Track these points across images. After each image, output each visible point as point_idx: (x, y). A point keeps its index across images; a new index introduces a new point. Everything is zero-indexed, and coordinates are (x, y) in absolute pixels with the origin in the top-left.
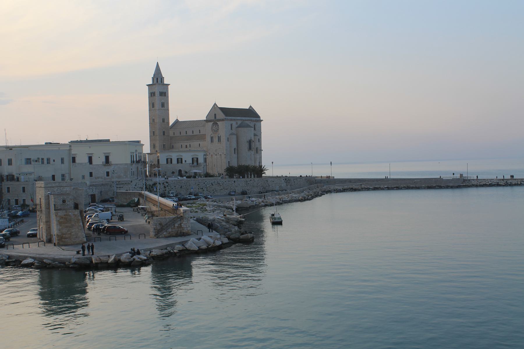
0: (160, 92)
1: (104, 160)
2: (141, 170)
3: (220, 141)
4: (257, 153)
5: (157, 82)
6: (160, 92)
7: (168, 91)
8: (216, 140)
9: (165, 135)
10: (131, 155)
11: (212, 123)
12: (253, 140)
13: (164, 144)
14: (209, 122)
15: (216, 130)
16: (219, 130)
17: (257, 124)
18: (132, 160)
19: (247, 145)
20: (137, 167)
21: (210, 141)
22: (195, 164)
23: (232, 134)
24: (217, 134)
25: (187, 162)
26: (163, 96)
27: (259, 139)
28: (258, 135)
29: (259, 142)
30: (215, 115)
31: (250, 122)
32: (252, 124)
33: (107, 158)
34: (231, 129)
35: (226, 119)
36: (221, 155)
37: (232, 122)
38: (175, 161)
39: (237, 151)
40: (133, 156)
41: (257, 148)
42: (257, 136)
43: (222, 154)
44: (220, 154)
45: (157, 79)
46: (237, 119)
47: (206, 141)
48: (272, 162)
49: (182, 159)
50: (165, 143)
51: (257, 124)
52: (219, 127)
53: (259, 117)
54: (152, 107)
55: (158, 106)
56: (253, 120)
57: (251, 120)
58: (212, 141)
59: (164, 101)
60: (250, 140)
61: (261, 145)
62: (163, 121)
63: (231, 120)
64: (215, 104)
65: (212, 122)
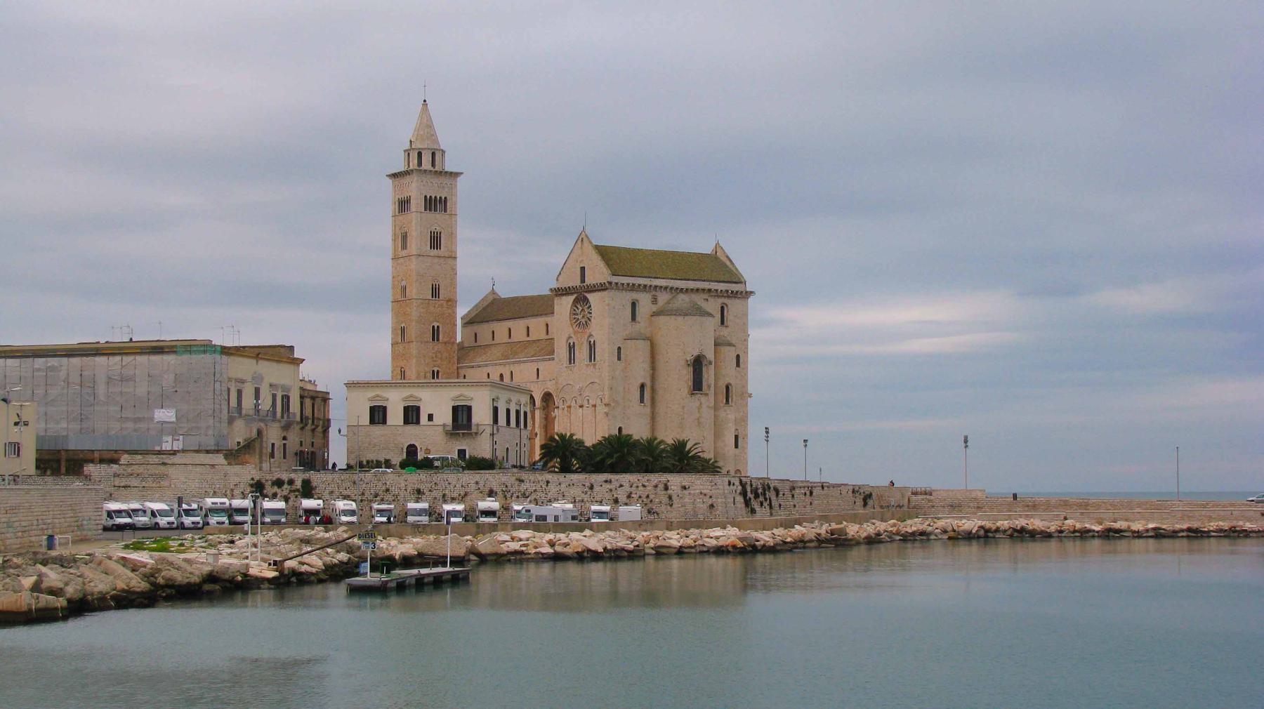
0: (426, 197)
2: (285, 445)
5: (420, 164)
6: (426, 197)
8: (582, 353)
9: (438, 340)
11: (571, 298)
12: (710, 355)
13: (436, 369)
14: (563, 295)
15: (583, 321)
16: (592, 320)
17: (734, 306)
19: (688, 374)
25: (437, 420)
26: (435, 210)
27: (738, 356)
28: (733, 342)
29: (738, 365)
31: (706, 296)
32: (713, 306)
36: (594, 406)
37: (635, 295)
38: (395, 416)
39: (648, 392)
41: (727, 388)
43: (599, 401)
45: (420, 154)
46: (656, 287)
47: (553, 359)
48: (805, 441)
49: (418, 408)
50: (439, 367)
52: (593, 315)
54: (400, 245)
55: (418, 242)
56: (717, 290)
57: (710, 290)
58: (571, 360)
59: (438, 229)
61: (744, 377)
62: (435, 291)
63: (633, 288)
65: (572, 294)
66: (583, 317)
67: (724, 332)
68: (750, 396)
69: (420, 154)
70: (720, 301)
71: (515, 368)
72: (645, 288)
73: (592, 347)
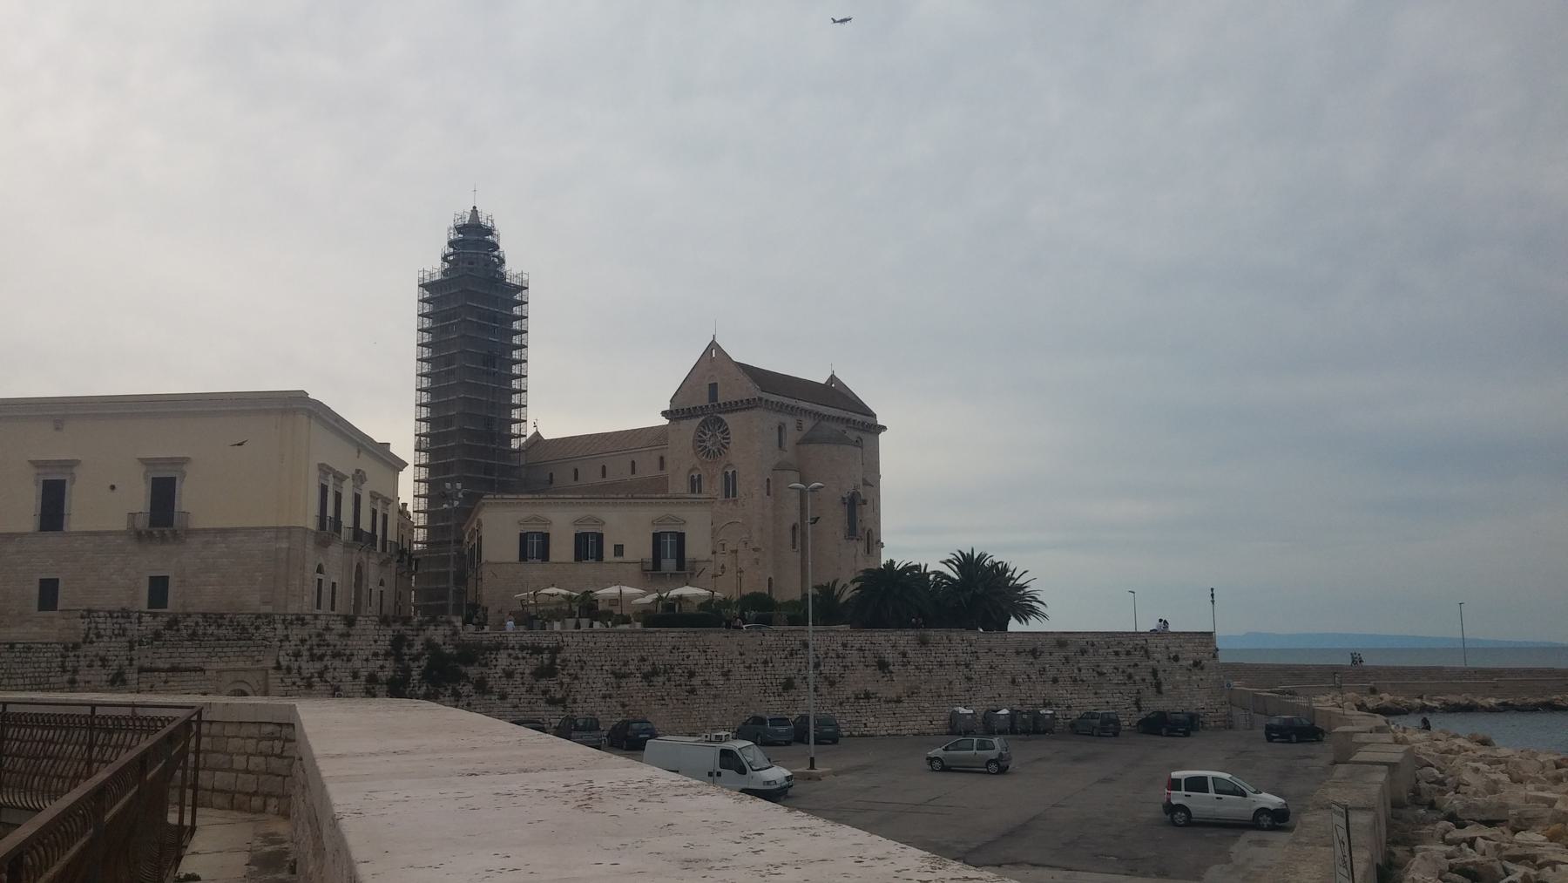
1: (139, 499)
3: (734, 495)
18: (330, 512)
22: (669, 564)
23: (780, 467)
24: (721, 466)
25: (628, 555)
33: (163, 493)
35: (763, 403)
38: (562, 549)
44: (729, 547)
49: (599, 538)
53: (874, 416)
60: (853, 494)
63: (781, 408)
64: (713, 345)
65: (697, 416)
66: (714, 444)
72: (792, 410)
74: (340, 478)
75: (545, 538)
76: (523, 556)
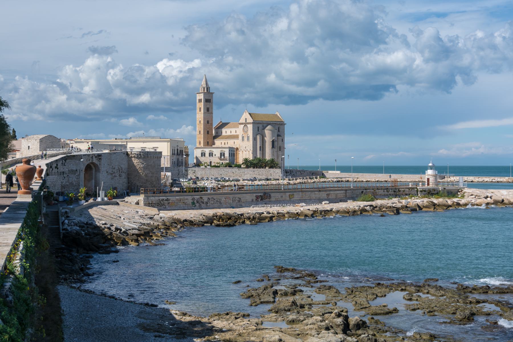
4: (280, 150)
5: (204, 91)
7: (212, 98)
8: (246, 139)
10: (173, 150)
17: (281, 127)
18: (174, 153)
20: (178, 159)
21: (241, 140)
25: (216, 156)
27: (282, 139)
29: (282, 141)
30: (246, 119)
31: (275, 125)
34: (258, 131)
38: (207, 155)
40: (175, 150)
42: (281, 136)
43: (250, 150)
44: (248, 150)
45: (204, 88)
49: (212, 153)
51: (281, 127)
58: (243, 140)
61: (284, 144)
62: (208, 122)
67: (279, 133)
68: (285, 148)
69: (204, 88)
70: (278, 126)
71: (228, 141)
73: (248, 138)
74: (175, 148)
75: (205, 153)
76: (202, 156)
